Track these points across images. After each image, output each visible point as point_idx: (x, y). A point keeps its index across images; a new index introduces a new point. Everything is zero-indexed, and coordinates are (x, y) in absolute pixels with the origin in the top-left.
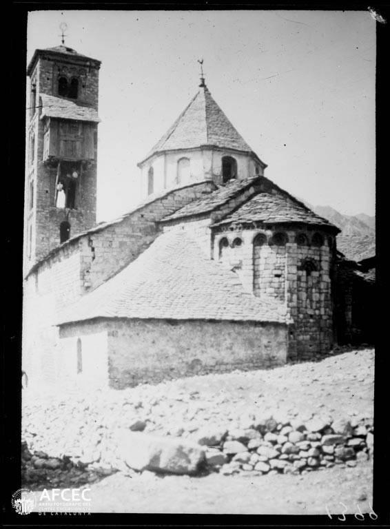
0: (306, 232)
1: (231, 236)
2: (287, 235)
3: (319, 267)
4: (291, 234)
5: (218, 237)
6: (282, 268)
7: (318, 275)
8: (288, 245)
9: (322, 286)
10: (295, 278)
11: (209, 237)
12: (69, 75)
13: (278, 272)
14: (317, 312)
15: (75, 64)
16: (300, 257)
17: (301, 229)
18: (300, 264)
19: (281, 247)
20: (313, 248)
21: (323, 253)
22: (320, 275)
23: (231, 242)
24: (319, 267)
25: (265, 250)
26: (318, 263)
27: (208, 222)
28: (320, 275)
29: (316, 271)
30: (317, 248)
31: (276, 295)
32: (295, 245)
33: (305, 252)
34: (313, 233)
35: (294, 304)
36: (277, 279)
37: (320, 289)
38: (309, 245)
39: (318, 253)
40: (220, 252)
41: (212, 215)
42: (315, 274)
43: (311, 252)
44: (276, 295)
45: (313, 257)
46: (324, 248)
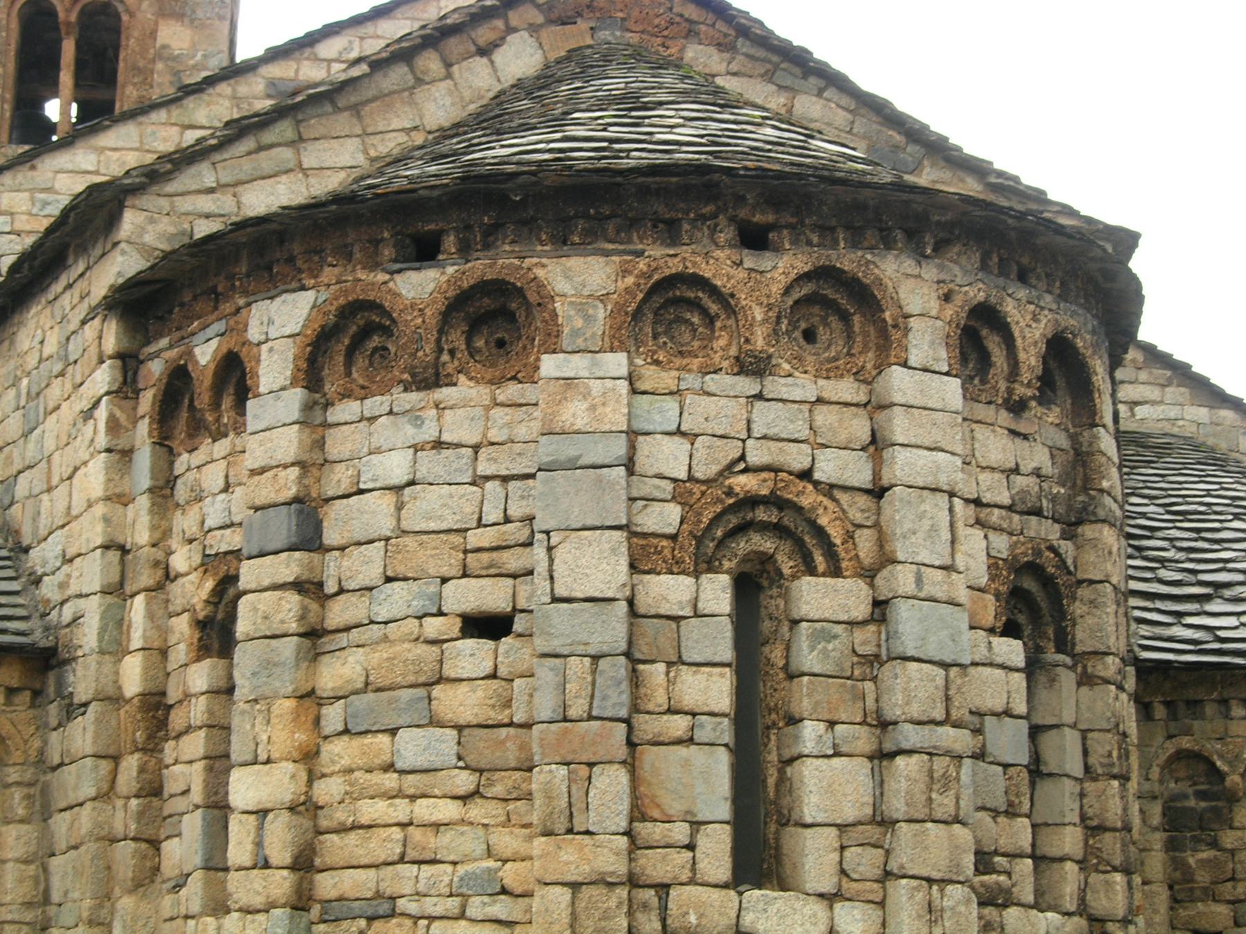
0: (721, 264)
1: (205, 353)
2: (546, 299)
3: (865, 543)
4: (582, 281)
7: (861, 610)
8: (550, 365)
9: (911, 691)
10: (611, 630)
11: (103, 378)
13: (490, 596)
16: (666, 457)
17: (670, 232)
18: (665, 517)
19: (511, 391)
20: (803, 387)
21: (900, 426)
22: (881, 608)
23: (203, 399)
24: (865, 543)
26: (857, 508)
28: (881, 608)
30: (846, 389)
31: (464, 781)
32: (617, 363)
33: (709, 421)
34: (783, 267)
35: (608, 856)
36: (473, 655)
37: (884, 725)
38: (753, 366)
39: (859, 428)
41: (130, 220)
42: (820, 598)
43: (766, 418)
44: (464, 781)
45: (797, 458)
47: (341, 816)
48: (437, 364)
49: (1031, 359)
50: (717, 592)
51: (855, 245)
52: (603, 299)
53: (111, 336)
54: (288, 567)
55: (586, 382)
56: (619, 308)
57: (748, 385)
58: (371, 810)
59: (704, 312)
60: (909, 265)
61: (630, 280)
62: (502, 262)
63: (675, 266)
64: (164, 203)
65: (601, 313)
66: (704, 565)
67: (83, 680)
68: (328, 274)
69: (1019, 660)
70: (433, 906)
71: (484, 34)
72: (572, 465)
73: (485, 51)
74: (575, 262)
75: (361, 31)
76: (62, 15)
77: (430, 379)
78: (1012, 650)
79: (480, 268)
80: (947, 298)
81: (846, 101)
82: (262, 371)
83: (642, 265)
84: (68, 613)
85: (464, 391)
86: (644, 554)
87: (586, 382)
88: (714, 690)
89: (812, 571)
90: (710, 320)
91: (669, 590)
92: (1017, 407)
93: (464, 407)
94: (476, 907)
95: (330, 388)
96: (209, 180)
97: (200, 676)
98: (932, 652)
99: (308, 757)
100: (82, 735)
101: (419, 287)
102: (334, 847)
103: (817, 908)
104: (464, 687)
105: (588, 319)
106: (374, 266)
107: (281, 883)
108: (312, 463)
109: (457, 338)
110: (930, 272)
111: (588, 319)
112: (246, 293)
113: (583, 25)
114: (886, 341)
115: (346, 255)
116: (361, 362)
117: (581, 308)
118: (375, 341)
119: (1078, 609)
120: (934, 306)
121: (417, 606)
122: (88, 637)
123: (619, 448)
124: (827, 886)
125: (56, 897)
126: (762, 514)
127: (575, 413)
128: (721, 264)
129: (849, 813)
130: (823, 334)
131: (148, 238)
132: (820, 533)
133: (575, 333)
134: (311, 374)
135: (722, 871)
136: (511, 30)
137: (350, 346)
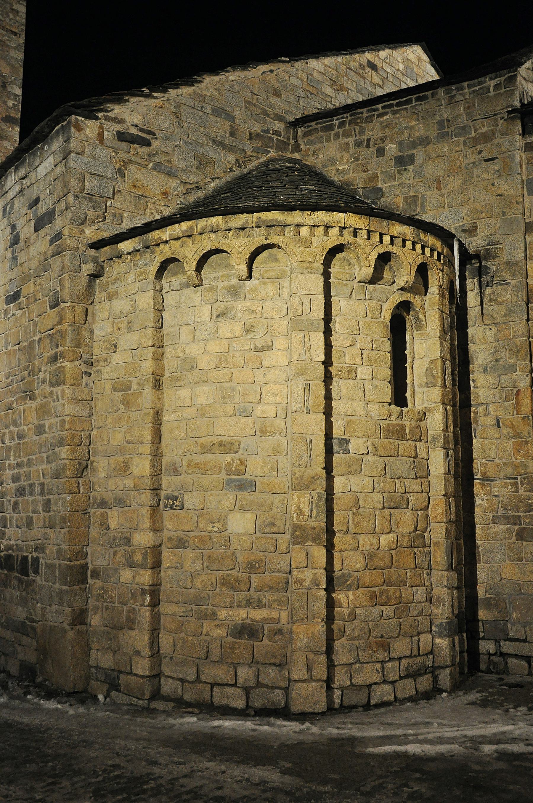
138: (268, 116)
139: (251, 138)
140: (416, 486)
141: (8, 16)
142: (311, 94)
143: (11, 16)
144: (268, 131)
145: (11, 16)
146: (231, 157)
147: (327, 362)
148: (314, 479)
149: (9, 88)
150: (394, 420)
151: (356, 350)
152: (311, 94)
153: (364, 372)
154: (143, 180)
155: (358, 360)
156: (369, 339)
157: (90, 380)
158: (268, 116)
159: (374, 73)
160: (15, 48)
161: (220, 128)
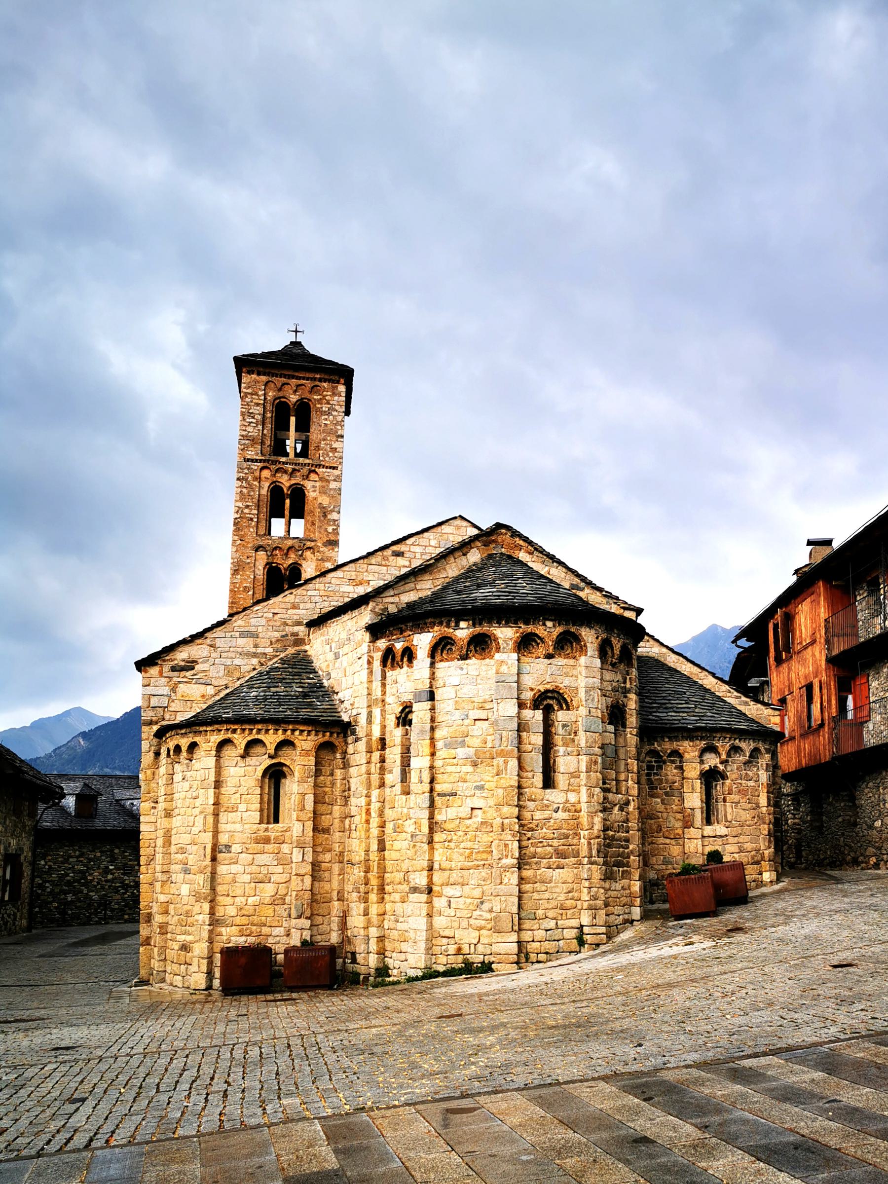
1: (399, 646)
2: (496, 639)
4: (506, 634)
5: (382, 644)
6: (487, 706)
8: (498, 656)
12: (294, 398)
13: (482, 714)
14: (572, 797)
15: (304, 378)
17: (527, 623)
23: (398, 658)
25: (451, 671)
27: (366, 616)
29: (568, 709)
40: (384, 677)
46: (583, 660)
47: (442, 770)
48: (467, 654)
49: (617, 652)
50: (539, 715)
51: (573, 625)
52: (511, 639)
53: (367, 636)
54: (427, 705)
55: (506, 659)
56: (516, 642)
57: (547, 661)
58: (449, 769)
59: (536, 642)
60: (588, 629)
61: (518, 635)
62: (485, 628)
63: (529, 630)
64: (380, 600)
65: (511, 643)
66: (536, 707)
67: (361, 731)
68: (436, 628)
69: (613, 731)
70: (467, 793)
71: (465, 550)
72: (503, 682)
73: (464, 555)
74: (504, 629)
75: (421, 536)
76: (285, 491)
77: (464, 657)
78: (611, 728)
79: (478, 629)
80: (597, 638)
81: (564, 570)
82: (418, 653)
83: (521, 630)
84: (354, 712)
85: (473, 661)
86: (521, 705)
87: (506, 659)
88: (538, 740)
89: (562, 709)
90: (538, 644)
91: (528, 713)
92: (613, 665)
93: (473, 664)
94: (478, 792)
95: (438, 658)
96: (392, 594)
97: (399, 732)
98: (592, 730)
99: (433, 754)
100: (362, 746)
101: (463, 632)
102: (439, 777)
103: (563, 794)
104: (475, 738)
105: (507, 644)
106: (448, 626)
107: (427, 787)
108: (433, 677)
109: (472, 648)
110: (593, 632)
111: (507, 644)
112: (411, 631)
113: (492, 546)
114: (583, 650)
115: (441, 624)
116: (445, 652)
117: (505, 641)
118: (449, 647)
119: (628, 716)
120: (594, 640)
121: (463, 717)
122: (363, 720)
123: (516, 678)
124: (566, 788)
125: (352, 789)
126: (549, 695)
127: (504, 669)
128: (540, 630)
129: (572, 770)
130: (566, 648)
131: (377, 610)
132: (565, 700)
133: (504, 648)
134: (432, 655)
135: (541, 785)
136: (472, 548)
137: (442, 648)
138: (287, 625)
139: (271, 643)
140: (279, 869)
141: (328, 455)
142: (328, 597)
143: (331, 454)
144: (287, 635)
145: (331, 454)
146: (255, 661)
147: (216, 804)
148: (206, 867)
149: (329, 517)
150: (262, 833)
151: (238, 795)
152: (328, 597)
153: (242, 807)
154: (188, 692)
155: (239, 801)
156: (245, 788)
157: (156, 811)
158: (287, 625)
159: (399, 558)
160: (335, 480)
161: (246, 644)
